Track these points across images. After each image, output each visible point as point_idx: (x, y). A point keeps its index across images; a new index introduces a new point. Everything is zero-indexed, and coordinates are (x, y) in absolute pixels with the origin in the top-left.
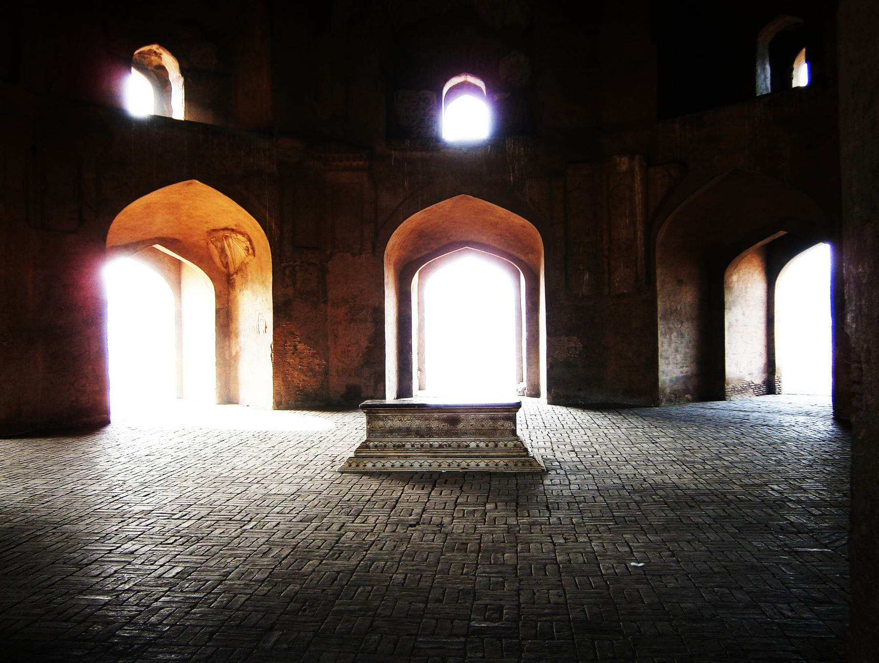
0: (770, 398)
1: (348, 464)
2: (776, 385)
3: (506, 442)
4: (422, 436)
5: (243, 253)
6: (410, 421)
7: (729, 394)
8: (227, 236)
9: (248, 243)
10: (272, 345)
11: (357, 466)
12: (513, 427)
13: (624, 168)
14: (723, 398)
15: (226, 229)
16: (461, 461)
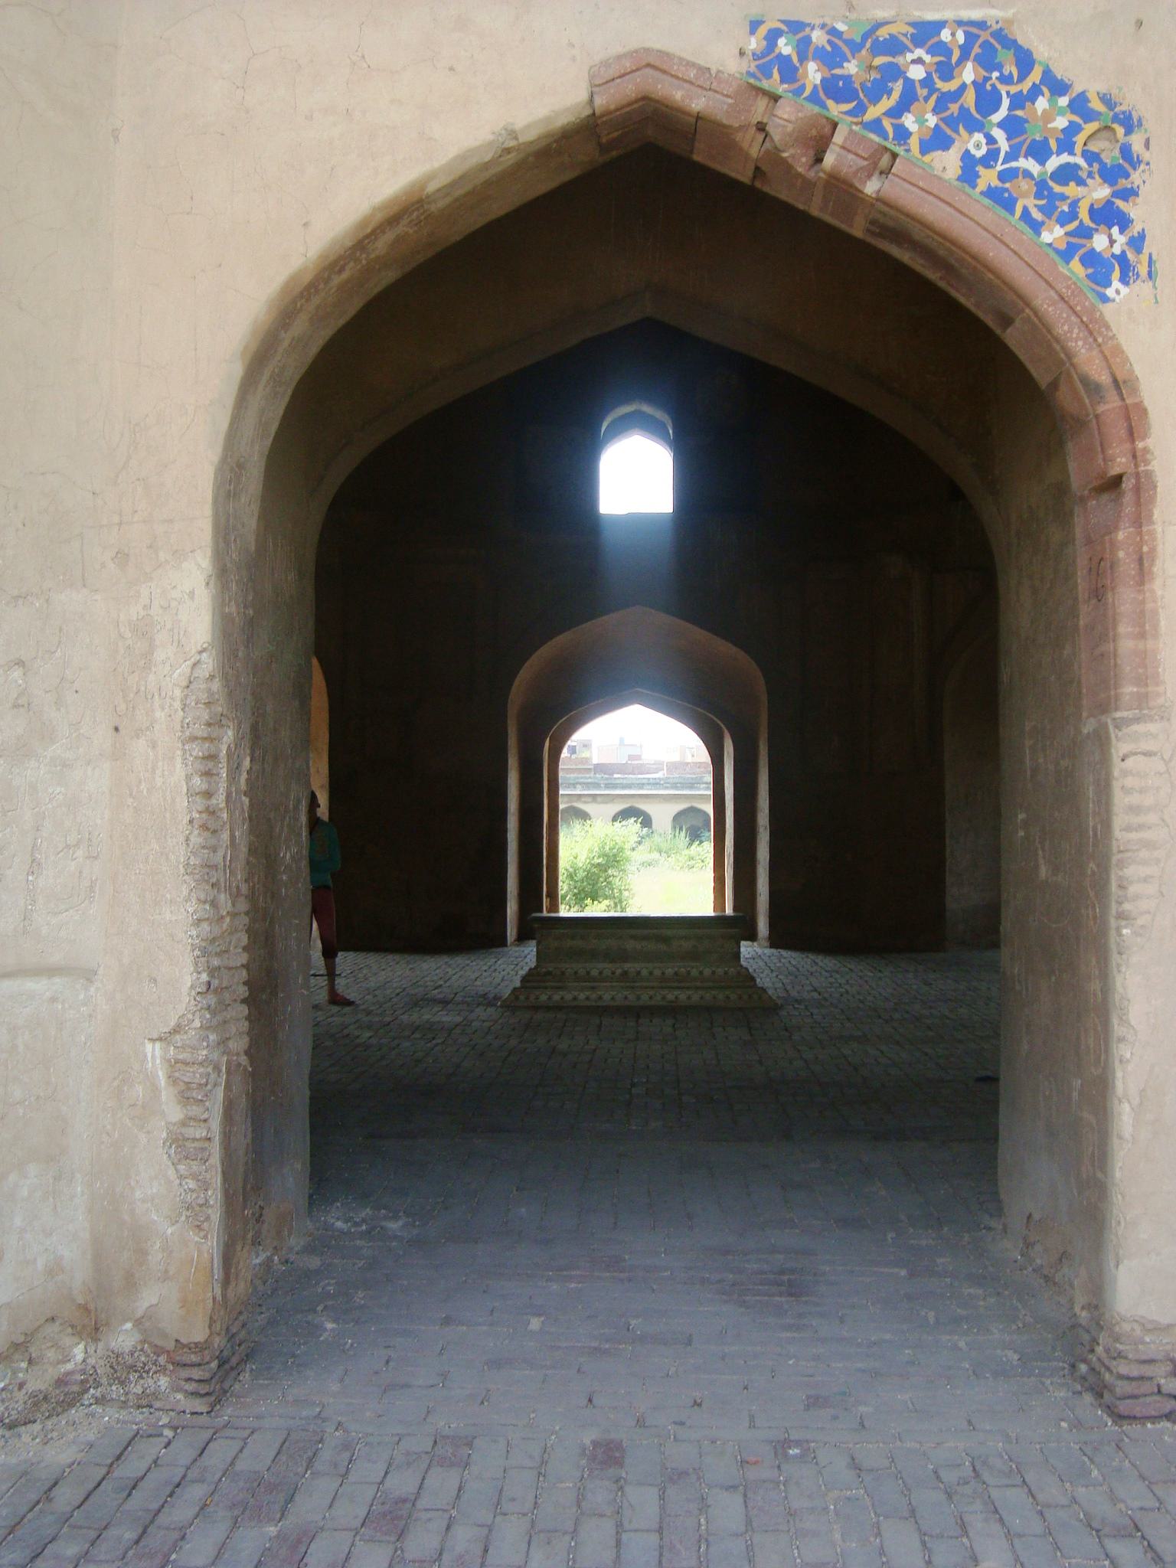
4: (613, 961)
11: (527, 998)
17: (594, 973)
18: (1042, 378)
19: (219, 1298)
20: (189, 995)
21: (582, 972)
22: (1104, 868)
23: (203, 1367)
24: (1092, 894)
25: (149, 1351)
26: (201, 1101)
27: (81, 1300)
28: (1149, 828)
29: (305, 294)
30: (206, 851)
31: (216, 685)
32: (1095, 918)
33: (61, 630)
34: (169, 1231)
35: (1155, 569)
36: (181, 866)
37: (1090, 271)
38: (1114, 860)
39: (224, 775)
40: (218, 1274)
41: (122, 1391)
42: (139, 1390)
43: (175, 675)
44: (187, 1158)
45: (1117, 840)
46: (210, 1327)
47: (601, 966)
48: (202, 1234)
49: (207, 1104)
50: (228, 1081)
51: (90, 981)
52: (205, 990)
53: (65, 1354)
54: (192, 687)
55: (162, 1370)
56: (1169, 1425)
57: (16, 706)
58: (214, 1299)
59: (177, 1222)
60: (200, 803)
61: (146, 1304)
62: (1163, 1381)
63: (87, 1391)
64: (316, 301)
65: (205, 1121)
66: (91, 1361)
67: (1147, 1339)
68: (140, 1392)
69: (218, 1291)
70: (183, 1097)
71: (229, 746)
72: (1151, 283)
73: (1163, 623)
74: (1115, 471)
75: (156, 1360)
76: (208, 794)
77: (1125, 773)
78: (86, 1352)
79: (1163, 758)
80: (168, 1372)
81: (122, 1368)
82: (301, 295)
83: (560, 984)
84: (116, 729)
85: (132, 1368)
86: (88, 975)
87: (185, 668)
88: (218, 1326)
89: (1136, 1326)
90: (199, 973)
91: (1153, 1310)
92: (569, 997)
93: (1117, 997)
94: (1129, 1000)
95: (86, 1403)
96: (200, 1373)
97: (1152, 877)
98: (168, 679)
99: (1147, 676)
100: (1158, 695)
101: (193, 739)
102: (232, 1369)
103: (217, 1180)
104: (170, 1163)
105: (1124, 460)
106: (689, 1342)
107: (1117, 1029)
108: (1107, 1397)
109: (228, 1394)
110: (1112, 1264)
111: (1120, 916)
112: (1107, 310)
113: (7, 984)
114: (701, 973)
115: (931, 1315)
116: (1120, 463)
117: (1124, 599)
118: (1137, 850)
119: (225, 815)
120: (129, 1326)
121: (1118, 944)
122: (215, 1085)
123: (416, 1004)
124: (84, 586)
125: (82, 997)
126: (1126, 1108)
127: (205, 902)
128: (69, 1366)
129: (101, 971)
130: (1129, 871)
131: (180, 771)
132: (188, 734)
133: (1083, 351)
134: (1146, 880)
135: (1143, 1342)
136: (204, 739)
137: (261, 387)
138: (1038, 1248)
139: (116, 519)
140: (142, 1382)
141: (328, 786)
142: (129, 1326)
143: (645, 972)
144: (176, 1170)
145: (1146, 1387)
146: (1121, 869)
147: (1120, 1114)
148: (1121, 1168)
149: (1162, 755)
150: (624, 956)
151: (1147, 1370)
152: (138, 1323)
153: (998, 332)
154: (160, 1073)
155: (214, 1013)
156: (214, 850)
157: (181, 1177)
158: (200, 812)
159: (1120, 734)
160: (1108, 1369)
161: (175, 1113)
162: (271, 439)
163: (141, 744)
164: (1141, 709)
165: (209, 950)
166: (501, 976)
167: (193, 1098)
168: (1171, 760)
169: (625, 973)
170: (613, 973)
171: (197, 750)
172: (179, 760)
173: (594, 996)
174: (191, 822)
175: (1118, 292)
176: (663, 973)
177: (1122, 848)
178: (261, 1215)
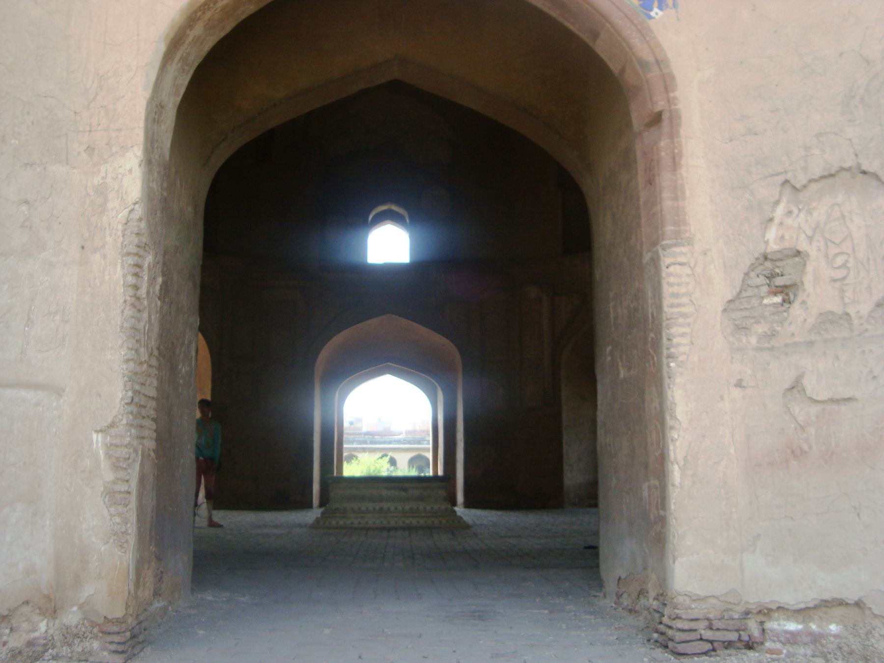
17: (363, 508)
18: (615, 68)
19: (132, 592)
20: (120, 403)
22: (659, 333)
23: (120, 634)
24: (651, 351)
25: (87, 625)
26: (126, 469)
27: (46, 592)
28: (684, 306)
29: (202, 8)
30: (133, 319)
31: (143, 225)
32: (654, 363)
33: (52, 186)
34: (103, 548)
35: (682, 162)
36: (118, 327)
37: (641, 2)
38: (664, 324)
39: (146, 279)
40: (132, 576)
41: (69, 650)
42: (80, 649)
43: (119, 217)
44: (115, 503)
45: (665, 312)
46: (126, 609)
48: (123, 550)
49: (129, 471)
50: (142, 461)
51: (60, 395)
52: (130, 401)
53: (34, 626)
54: (128, 224)
55: (96, 637)
56: (707, 658)
57: (22, 226)
58: (129, 593)
59: (108, 542)
60: (131, 292)
61: (86, 595)
62: (703, 632)
63: (47, 651)
64: (208, 14)
65: (127, 481)
66: (51, 632)
67: (693, 606)
68: (81, 651)
69: (132, 588)
70: (114, 466)
71: (150, 263)
72: (674, 10)
73: (687, 192)
74: (658, 109)
75: (91, 631)
76: (136, 287)
77: (669, 275)
78: (48, 626)
79: (690, 267)
80: (99, 638)
81: (70, 636)
82: (199, 9)
84: (83, 248)
85: (76, 636)
86: (59, 392)
87: (125, 213)
88: (131, 610)
89: (686, 598)
90: (127, 391)
91: (696, 588)
92: (348, 522)
93: (668, 403)
94: (675, 404)
95: (46, 658)
96: (119, 638)
97: (685, 333)
98: (115, 219)
99: (680, 221)
100: (686, 231)
101: (128, 254)
102: (139, 643)
103: (134, 519)
104: (105, 506)
105: (662, 103)
106: (420, 636)
107: (669, 422)
108: (670, 644)
109: (136, 657)
110: (671, 562)
111: (669, 356)
112: (651, 23)
113: (8, 393)
114: (425, 508)
115: (564, 626)
116: (660, 104)
117: (665, 179)
118: (677, 318)
119: (146, 303)
120: (75, 608)
121: (668, 373)
122: (134, 461)
124: (67, 164)
125: (55, 404)
126: (676, 467)
127: (132, 349)
128: (36, 634)
129: (67, 390)
130: (674, 330)
131: (119, 271)
132: (125, 251)
133: (639, 44)
134: (683, 335)
135: (691, 609)
136: (136, 254)
137: (176, 60)
138: (625, 596)
139: (88, 128)
140: (82, 644)
142: (75, 608)
143: (392, 509)
144: (108, 510)
145: (693, 636)
146: (668, 329)
147: (673, 471)
148: (674, 503)
149: (689, 265)
150: (381, 499)
151: (693, 625)
152: (81, 607)
153: (591, 44)
154: (101, 452)
155: (135, 417)
156: (139, 321)
157: (111, 515)
158: (131, 296)
159: (665, 253)
160: (670, 627)
161: (109, 475)
162: (180, 97)
163: (97, 256)
164: (676, 239)
165: (133, 377)
167: (120, 467)
168: (695, 265)
169: (381, 509)
171: (131, 260)
172: (119, 266)
174: (125, 301)
175: (657, 14)
177: (669, 317)
178: (161, 578)
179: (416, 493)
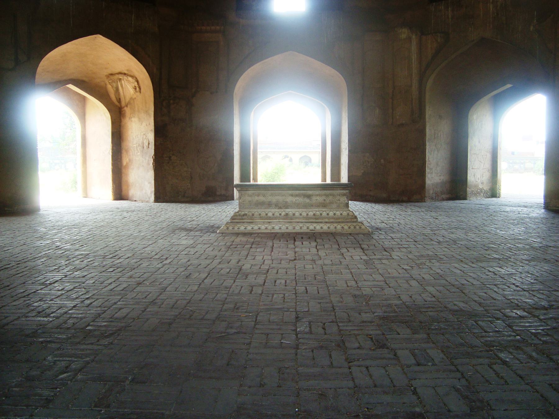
0: (494, 199)
1: (225, 228)
2: (497, 191)
3: (341, 212)
4: (280, 208)
5: (132, 91)
6: (271, 197)
7: (469, 195)
8: (121, 79)
9: (136, 83)
10: (154, 156)
12: (346, 201)
13: (404, 36)
14: (465, 198)
15: (120, 73)
16: (309, 225)
17: (270, 214)
21: (263, 214)
47: (273, 210)
83: (251, 221)
92: (256, 227)
114: (328, 214)
123: (174, 231)
141: (153, 130)
143: (297, 214)
150: (286, 206)
166: (226, 215)
169: (287, 214)
170: (280, 214)
173: (270, 227)
176: (307, 215)
179: (320, 199)
